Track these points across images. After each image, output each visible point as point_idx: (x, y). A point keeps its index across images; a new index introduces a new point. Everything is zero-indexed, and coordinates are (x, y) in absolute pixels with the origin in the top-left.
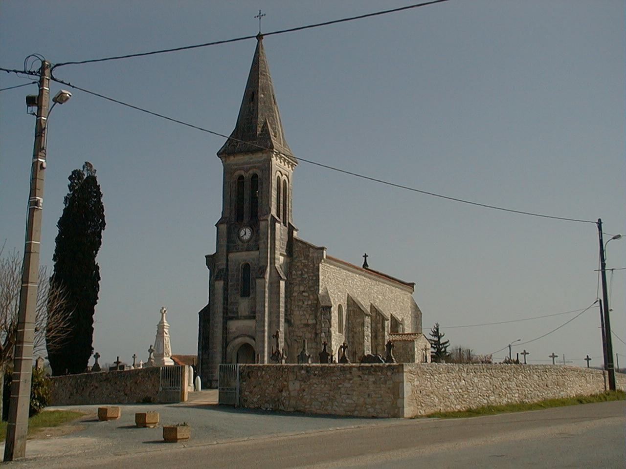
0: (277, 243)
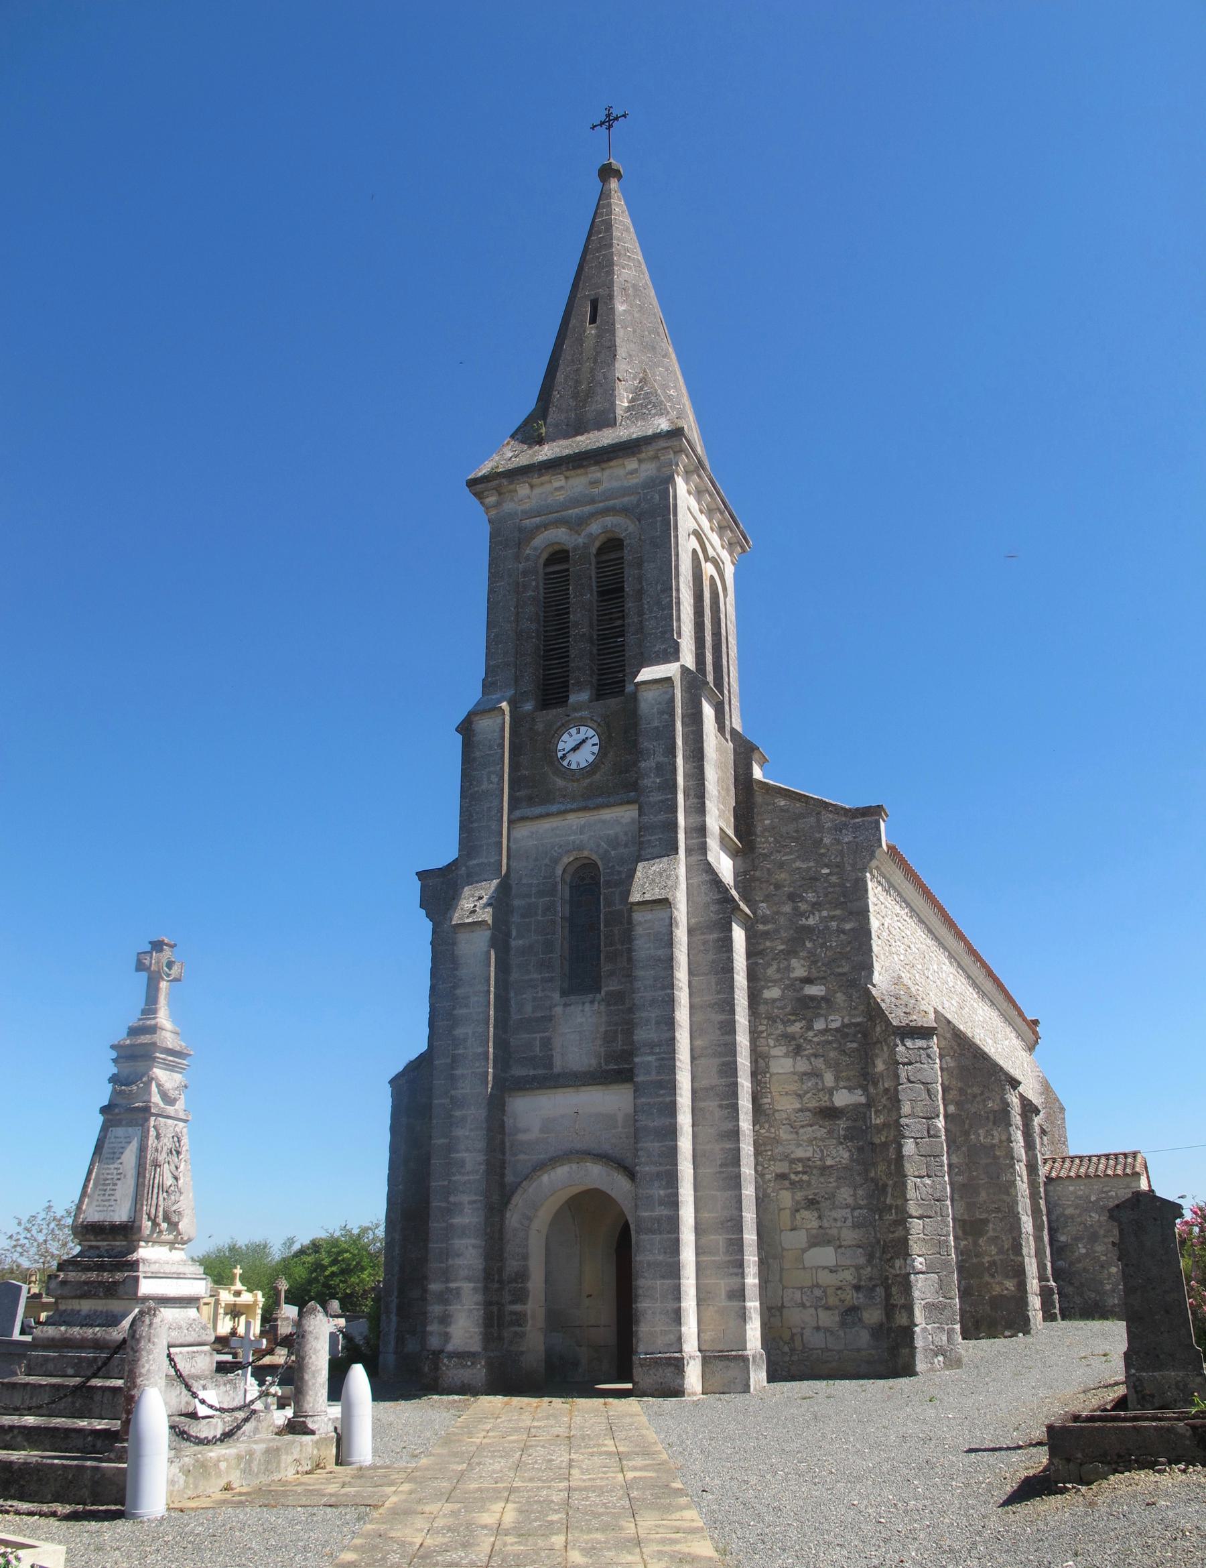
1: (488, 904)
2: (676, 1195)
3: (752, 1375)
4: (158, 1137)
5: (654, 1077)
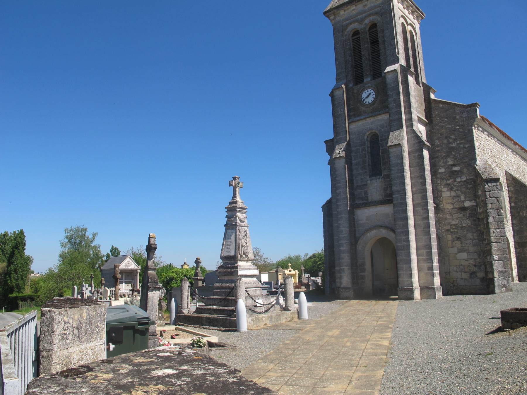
0: (413, 100)
1: (344, 151)
2: (409, 238)
3: (436, 294)
4: (240, 232)
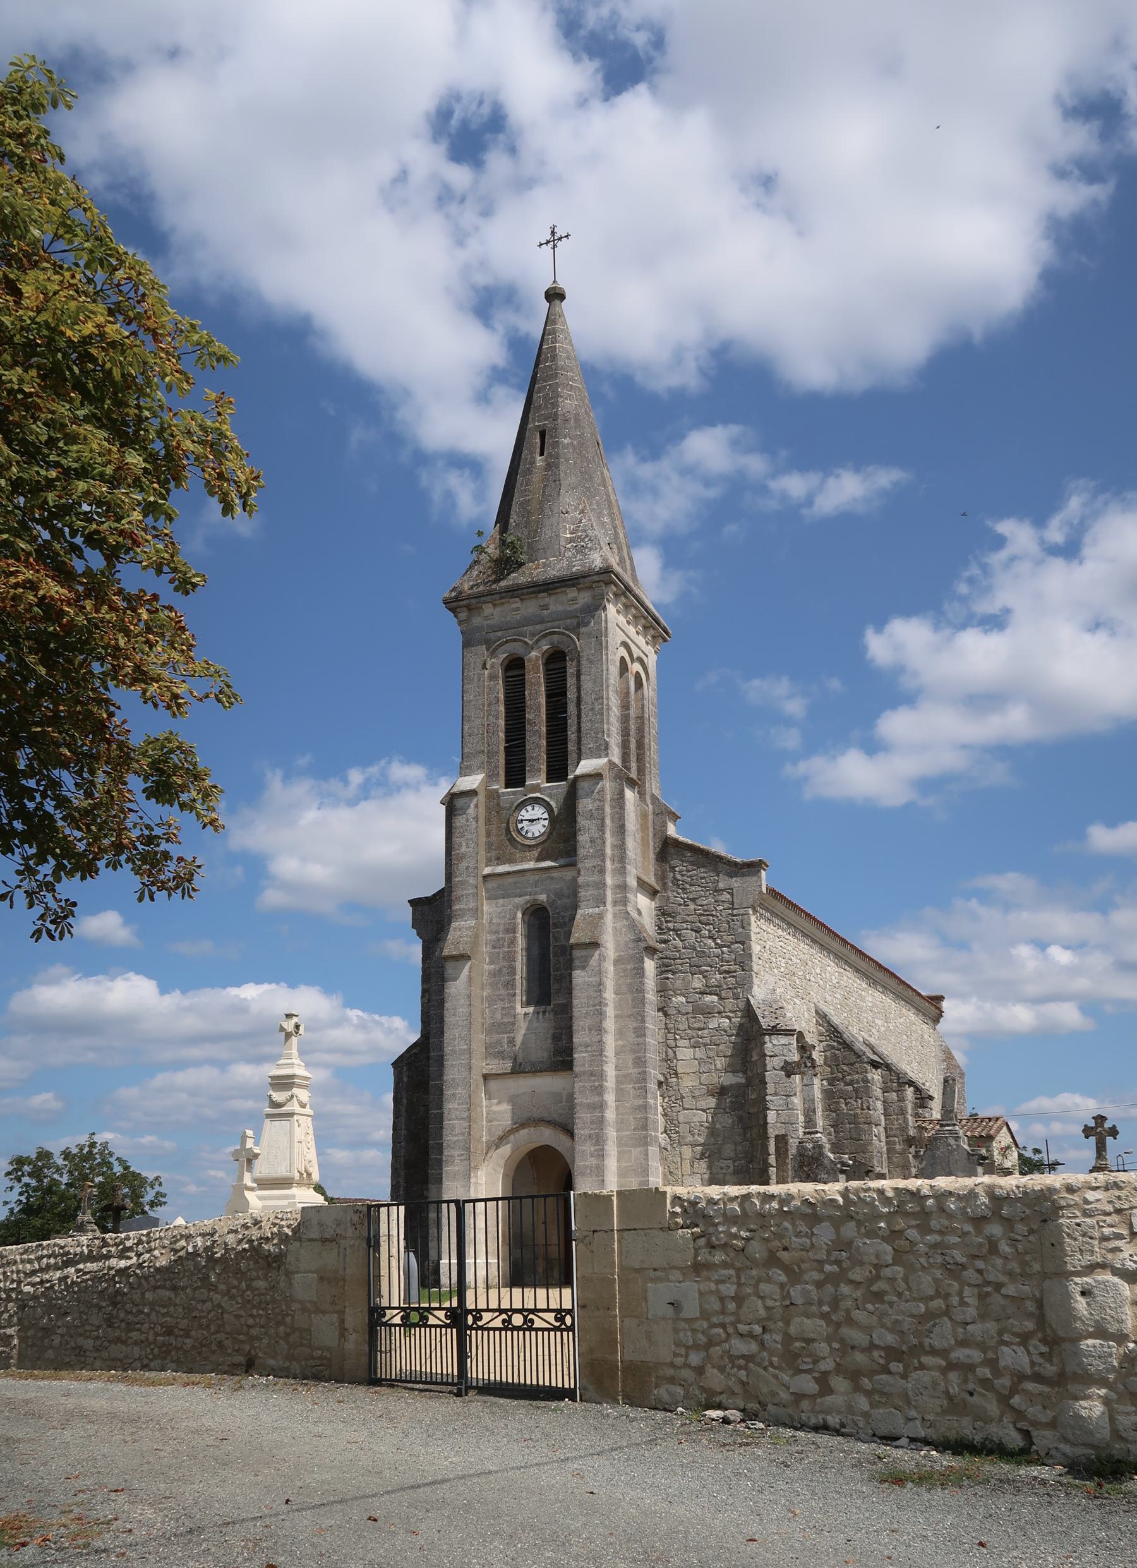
5: (587, 1068)
